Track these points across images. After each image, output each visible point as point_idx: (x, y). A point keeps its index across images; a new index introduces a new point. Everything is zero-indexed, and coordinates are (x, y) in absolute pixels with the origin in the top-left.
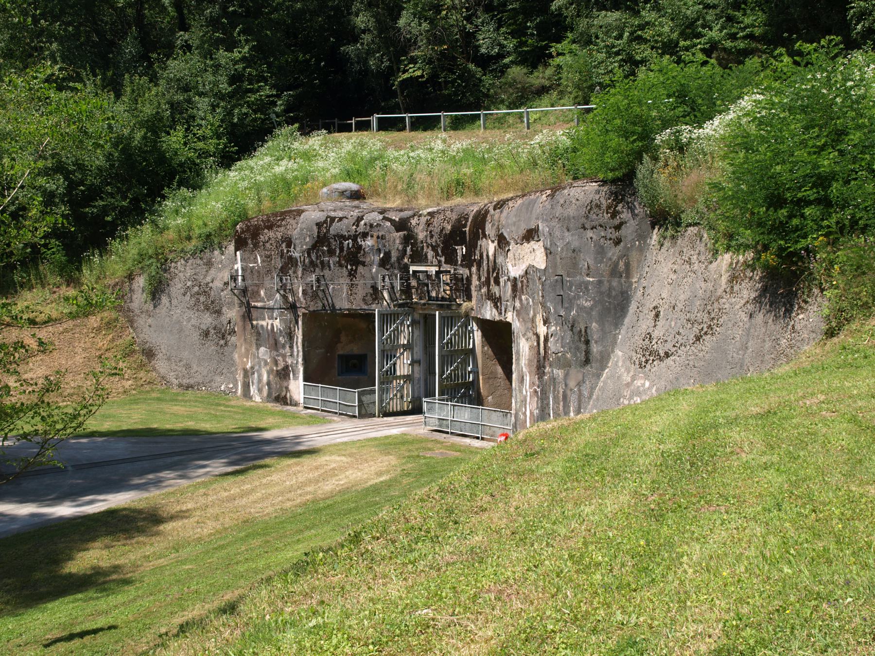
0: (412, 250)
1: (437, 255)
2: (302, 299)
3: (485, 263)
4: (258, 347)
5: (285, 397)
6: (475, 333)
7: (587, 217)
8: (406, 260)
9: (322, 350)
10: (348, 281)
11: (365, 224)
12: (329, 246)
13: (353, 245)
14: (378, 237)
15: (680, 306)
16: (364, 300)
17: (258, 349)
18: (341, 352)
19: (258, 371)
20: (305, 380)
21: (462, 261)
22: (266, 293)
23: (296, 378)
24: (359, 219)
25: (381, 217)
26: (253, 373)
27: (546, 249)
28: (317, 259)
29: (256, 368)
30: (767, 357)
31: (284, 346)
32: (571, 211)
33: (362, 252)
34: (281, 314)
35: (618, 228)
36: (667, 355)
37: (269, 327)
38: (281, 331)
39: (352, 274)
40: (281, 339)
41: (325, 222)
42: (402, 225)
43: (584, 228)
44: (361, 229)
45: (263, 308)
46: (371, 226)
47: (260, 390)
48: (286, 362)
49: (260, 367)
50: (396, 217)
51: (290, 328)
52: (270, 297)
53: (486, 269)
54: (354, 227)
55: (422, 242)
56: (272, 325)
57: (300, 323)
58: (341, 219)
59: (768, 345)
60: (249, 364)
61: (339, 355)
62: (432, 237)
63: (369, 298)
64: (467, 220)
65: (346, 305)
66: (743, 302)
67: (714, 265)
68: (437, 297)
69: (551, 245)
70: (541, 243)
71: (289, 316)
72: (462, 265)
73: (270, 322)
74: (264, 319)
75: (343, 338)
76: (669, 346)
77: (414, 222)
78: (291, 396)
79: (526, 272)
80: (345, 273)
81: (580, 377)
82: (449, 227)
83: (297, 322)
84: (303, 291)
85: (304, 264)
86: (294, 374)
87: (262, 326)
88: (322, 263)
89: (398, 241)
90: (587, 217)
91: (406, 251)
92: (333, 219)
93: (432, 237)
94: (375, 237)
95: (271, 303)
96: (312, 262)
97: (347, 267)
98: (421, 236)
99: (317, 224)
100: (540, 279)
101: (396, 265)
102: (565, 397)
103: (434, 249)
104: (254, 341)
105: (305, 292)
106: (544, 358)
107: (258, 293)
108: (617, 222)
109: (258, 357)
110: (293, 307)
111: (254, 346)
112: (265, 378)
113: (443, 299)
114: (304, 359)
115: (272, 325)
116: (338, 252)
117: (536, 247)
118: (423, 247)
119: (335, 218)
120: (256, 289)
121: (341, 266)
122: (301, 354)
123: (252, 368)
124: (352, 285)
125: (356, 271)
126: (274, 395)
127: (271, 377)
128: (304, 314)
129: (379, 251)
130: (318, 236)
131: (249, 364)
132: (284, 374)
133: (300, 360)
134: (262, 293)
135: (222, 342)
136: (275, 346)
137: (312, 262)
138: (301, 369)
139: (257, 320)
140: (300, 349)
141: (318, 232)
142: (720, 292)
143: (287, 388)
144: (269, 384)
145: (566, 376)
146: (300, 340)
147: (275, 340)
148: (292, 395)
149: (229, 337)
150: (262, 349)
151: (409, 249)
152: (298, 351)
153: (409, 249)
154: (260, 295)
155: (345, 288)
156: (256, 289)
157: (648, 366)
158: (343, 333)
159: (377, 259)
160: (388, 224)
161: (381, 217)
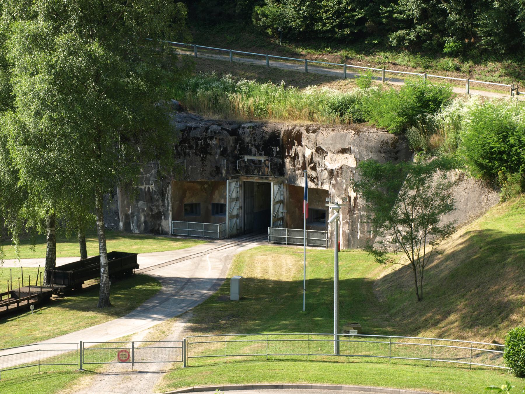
0: (240, 146)
1: (259, 150)
3: (301, 159)
4: (137, 201)
5: (158, 229)
7: (382, 148)
8: (236, 152)
9: (178, 202)
10: (201, 163)
11: (211, 132)
12: (189, 143)
13: (204, 143)
14: (220, 139)
17: (137, 202)
18: (186, 203)
19: (136, 216)
20: (173, 220)
21: (276, 155)
23: (166, 218)
24: (207, 129)
25: (220, 128)
26: (134, 217)
27: (356, 159)
28: (181, 150)
29: (136, 213)
30: (477, 208)
31: (157, 200)
32: (373, 144)
33: (210, 147)
35: (397, 153)
37: (146, 190)
39: (203, 160)
40: (155, 196)
41: (186, 129)
42: (233, 132)
43: (380, 152)
44: (209, 134)
46: (215, 133)
47: (138, 227)
48: (159, 209)
49: (139, 213)
50: (229, 128)
51: (162, 190)
52: (147, 171)
53: (301, 162)
54: (205, 133)
55: (248, 143)
56: (149, 188)
58: (195, 128)
59: (477, 204)
60: (130, 211)
62: (255, 140)
64: (279, 133)
66: (464, 188)
69: (360, 157)
70: (353, 156)
72: (276, 157)
74: (142, 185)
75: (188, 194)
77: (241, 131)
78: (162, 229)
79: (341, 168)
80: (199, 158)
82: (268, 136)
85: (173, 153)
86: (164, 216)
87: (141, 189)
88: (185, 153)
89: (231, 142)
90: (382, 148)
91: (236, 147)
92: (190, 128)
93: (255, 140)
94: (218, 140)
96: (178, 152)
97: (200, 156)
98: (247, 139)
99: (181, 131)
100: (351, 171)
101: (230, 154)
103: (257, 147)
106: (354, 207)
108: (396, 150)
109: (137, 207)
111: (134, 201)
112: (143, 219)
114: (173, 208)
115: (149, 188)
116: (195, 147)
118: (248, 145)
119: (191, 127)
121: (197, 155)
122: (170, 204)
123: (132, 213)
125: (206, 158)
126: (149, 229)
127: (147, 219)
129: (220, 147)
130: (182, 138)
131: (130, 211)
132: (159, 216)
137: (178, 152)
141: (182, 136)
143: (160, 225)
144: (145, 222)
146: (170, 197)
147: (151, 197)
150: (141, 203)
151: (238, 146)
152: (168, 204)
153: (238, 146)
154: (139, 170)
158: (188, 192)
159: (219, 151)
160: (225, 132)
161: (220, 128)
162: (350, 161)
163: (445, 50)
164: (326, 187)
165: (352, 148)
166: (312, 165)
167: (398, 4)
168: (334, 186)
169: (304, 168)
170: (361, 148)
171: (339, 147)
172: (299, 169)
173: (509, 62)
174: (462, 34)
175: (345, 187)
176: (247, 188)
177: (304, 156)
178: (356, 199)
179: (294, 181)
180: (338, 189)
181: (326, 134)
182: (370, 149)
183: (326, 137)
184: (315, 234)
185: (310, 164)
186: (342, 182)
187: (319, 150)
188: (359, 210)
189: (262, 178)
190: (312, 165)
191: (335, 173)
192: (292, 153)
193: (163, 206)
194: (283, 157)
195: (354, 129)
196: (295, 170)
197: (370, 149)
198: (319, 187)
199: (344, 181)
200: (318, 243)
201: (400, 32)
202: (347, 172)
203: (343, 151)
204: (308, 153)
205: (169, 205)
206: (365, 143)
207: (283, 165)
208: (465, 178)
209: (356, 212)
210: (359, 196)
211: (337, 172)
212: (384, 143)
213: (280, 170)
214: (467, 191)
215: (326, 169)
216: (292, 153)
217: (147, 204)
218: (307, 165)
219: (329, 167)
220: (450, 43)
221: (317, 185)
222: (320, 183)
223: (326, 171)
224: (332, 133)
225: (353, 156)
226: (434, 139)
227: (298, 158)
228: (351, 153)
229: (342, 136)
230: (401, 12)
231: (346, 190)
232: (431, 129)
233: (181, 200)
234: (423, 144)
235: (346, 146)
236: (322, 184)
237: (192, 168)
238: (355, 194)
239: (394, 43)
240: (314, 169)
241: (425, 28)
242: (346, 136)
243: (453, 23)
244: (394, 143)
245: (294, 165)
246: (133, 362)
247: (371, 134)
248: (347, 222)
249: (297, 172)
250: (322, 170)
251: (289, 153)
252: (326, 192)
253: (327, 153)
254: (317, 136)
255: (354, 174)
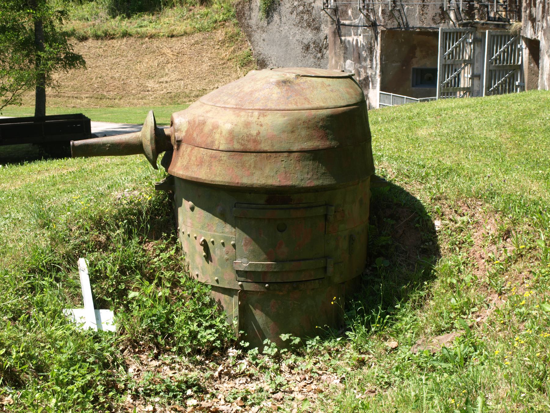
2: (381, 18)
4: (345, 59)
6: (524, 50)
16: (433, 19)
17: (345, 61)
18: (416, 66)
20: (382, 89)
22: (352, 12)
23: (374, 87)
31: (365, 60)
34: (364, 31)
37: (354, 43)
38: (363, 46)
40: (363, 53)
45: (350, 25)
48: (367, 73)
51: (371, 44)
52: (355, 16)
56: (357, 40)
57: (379, 39)
61: (413, 69)
63: (437, 18)
65: (418, 24)
68: (495, 18)
71: (370, 33)
73: (355, 38)
74: (350, 35)
75: (418, 53)
78: (369, 103)
83: (376, 39)
84: (382, 10)
86: (373, 84)
87: (349, 41)
95: (356, 21)
104: (342, 55)
105: (383, 12)
107: (346, 12)
110: (374, 25)
111: (342, 59)
113: (500, 19)
114: (382, 71)
115: (357, 40)
120: (345, 8)
122: (379, 66)
124: (424, 5)
128: (382, 31)
133: (378, 72)
134: (350, 12)
135: (319, 55)
136: (359, 59)
138: (378, 79)
139: (345, 36)
140: (379, 62)
148: (371, 102)
149: (325, 50)
150: (349, 62)
152: (377, 64)
154: (348, 14)
155: (418, 9)
156: (345, 8)
158: (418, 49)
193: (371, 67)
205: (374, 70)
217: (355, 64)
233: (406, 61)
237: (408, 8)
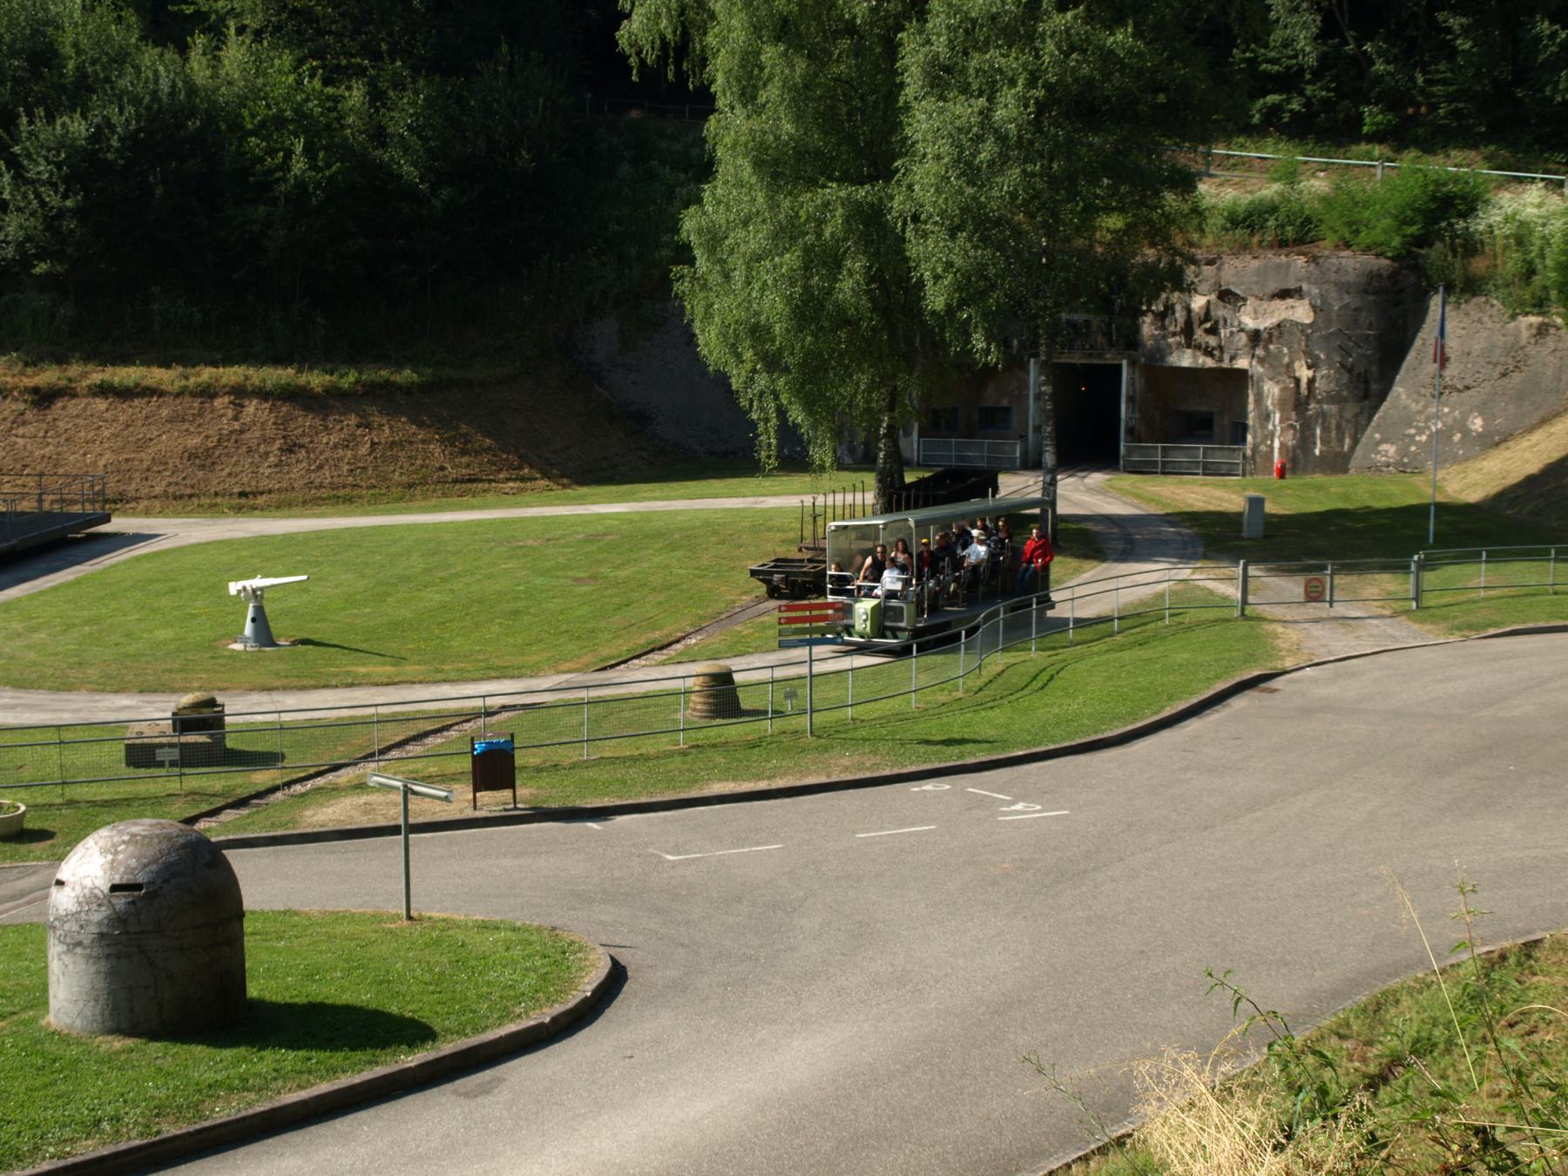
3: (1180, 315)
15: (1475, 353)
23: (908, 434)
32: (1351, 277)
36: (1468, 388)
43: (1366, 292)
67: (1512, 324)
69: (1323, 302)
70: (1306, 301)
76: (1468, 382)
79: (1279, 325)
81: (1357, 409)
102: (1338, 427)
106: (1308, 397)
117: (1297, 303)
142: (1523, 343)
145: (1341, 411)
157: (1444, 397)
162: (1302, 312)
163: (1365, 129)
164: (1242, 363)
165: (1305, 287)
166: (1208, 325)
167: (1266, 46)
168: (1261, 361)
169: (1188, 330)
170: (1326, 286)
171: (1273, 286)
172: (1174, 334)
173: (1493, 148)
174: (1394, 101)
175: (1286, 360)
176: (1062, 376)
177: (1189, 310)
178: (1311, 381)
179: (1163, 358)
180: (1272, 366)
181: (1240, 266)
182: (1344, 288)
183: (1238, 270)
184: (1218, 453)
185: (1202, 323)
186: (1280, 351)
187: (1226, 296)
188: (1319, 402)
189: (1090, 355)
190: (1208, 325)
191: (1265, 335)
192: (1158, 307)
194: (1137, 314)
195: (1305, 254)
196: (1164, 337)
197: (1344, 288)
198: (1226, 364)
199: (1285, 350)
200: (1225, 469)
201: (1272, 98)
202: (1291, 333)
203: (1284, 294)
204: (1198, 302)
206: (1333, 276)
207: (1137, 330)
208: (1552, 331)
209: (1312, 406)
210: (1318, 375)
211: (1270, 335)
212: (1373, 276)
213: (1132, 341)
214: (1558, 354)
215: (1242, 330)
216: (1158, 307)
218: (1195, 326)
219: (1250, 323)
220: (1372, 116)
221: (1221, 360)
222: (1226, 357)
223: (1243, 335)
224: (1255, 264)
225: (1306, 301)
226: (1479, 265)
227: (1173, 312)
228: (1301, 297)
229: (1279, 267)
230: (1272, 61)
231: (1289, 366)
232: (1471, 247)
234: (1457, 274)
235: (1292, 285)
236: (1232, 358)
238: (1310, 373)
239: (1256, 119)
240: (1213, 331)
241: (1321, 89)
242: (1288, 266)
243: (1379, 79)
244: (1393, 276)
245: (1163, 328)
246: (1331, 603)
247: (1344, 261)
248: (1292, 426)
249: (1171, 340)
250: (1232, 333)
251: (1149, 305)
252: (1243, 373)
253: (1245, 300)
254: (1218, 269)
255: (1308, 336)
